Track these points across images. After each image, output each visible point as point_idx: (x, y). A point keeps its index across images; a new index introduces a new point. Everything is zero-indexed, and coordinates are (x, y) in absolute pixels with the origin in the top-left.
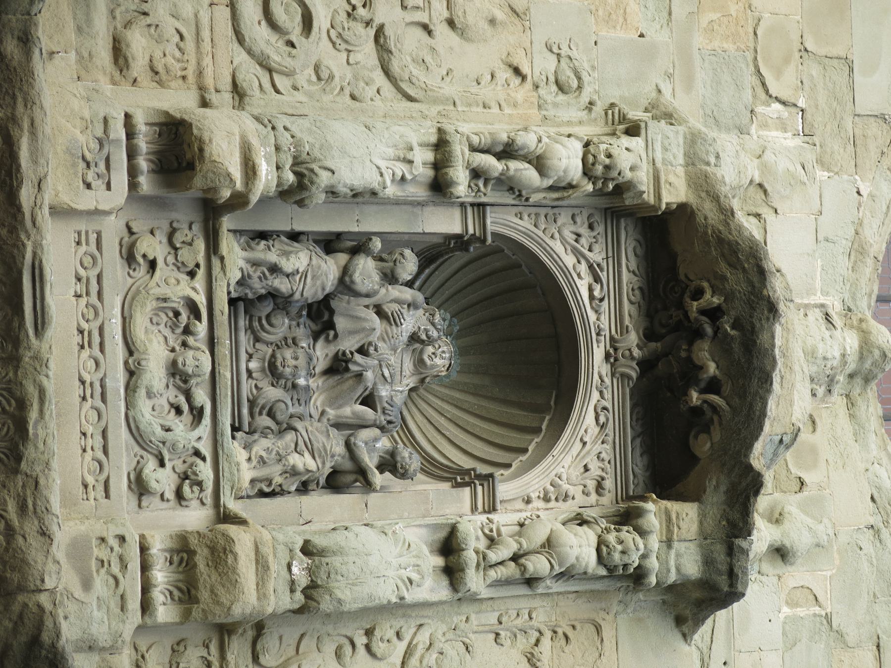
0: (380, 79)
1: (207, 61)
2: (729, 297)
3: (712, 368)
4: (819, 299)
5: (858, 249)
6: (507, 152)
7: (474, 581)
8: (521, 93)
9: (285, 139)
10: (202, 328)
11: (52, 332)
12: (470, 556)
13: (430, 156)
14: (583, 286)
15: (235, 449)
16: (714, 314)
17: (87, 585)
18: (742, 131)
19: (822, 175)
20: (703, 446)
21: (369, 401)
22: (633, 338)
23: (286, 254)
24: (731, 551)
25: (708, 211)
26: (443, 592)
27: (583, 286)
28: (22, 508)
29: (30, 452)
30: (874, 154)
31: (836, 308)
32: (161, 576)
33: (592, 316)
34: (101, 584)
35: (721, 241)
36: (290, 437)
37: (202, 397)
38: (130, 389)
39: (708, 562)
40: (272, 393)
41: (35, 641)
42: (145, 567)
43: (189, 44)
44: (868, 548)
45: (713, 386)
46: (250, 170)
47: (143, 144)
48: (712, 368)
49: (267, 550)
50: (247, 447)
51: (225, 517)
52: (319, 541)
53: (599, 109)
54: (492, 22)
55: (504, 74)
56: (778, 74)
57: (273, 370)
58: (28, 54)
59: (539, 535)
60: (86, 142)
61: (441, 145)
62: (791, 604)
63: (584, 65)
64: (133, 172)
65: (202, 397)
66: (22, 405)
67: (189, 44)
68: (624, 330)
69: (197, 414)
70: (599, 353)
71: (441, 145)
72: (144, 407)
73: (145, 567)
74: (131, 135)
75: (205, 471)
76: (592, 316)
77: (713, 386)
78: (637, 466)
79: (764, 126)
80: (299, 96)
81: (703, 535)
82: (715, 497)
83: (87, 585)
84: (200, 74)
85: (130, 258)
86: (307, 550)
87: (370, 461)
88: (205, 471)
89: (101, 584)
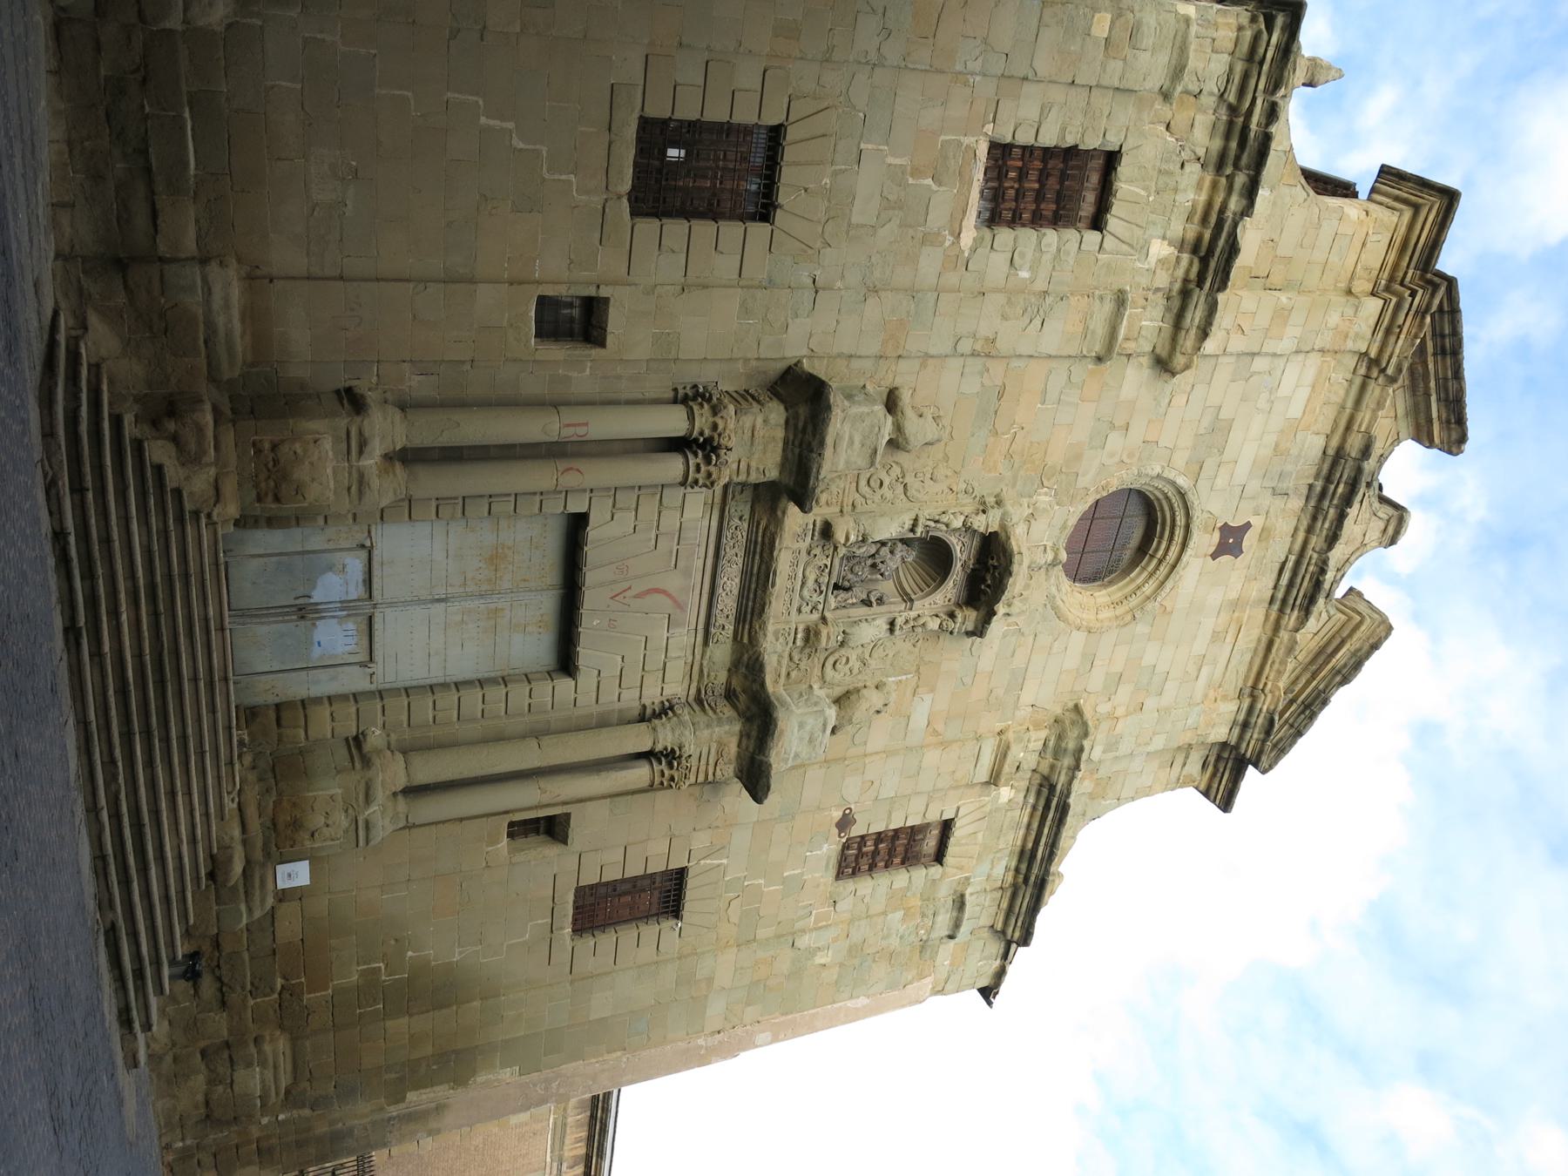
0: (903, 496)
1: (845, 499)
2: (1000, 564)
3: (989, 582)
4: (1045, 543)
5: (1064, 527)
6: (937, 522)
7: (897, 632)
8: (951, 497)
9: (862, 528)
10: (827, 571)
11: (777, 588)
12: (898, 627)
13: (912, 522)
14: (958, 549)
15: (831, 599)
16: (995, 568)
17: (777, 640)
18: (1030, 497)
19: (1057, 507)
20: (983, 598)
21: (882, 575)
22: (972, 561)
23: (860, 547)
24: (983, 626)
25: (1003, 535)
26: (888, 634)
27: (958, 549)
28: (760, 627)
29: (764, 616)
30: (1079, 498)
31: (1049, 544)
32: (799, 636)
33: (959, 555)
34: (781, 640)
35: (1003, 546)
36: (850, 593)
37: (824, 588)
38: (802, 587)
39: (976, 627)
40: (850, 576)
41: (757, 659)
42: (796, 633)
43: (841, 495)
44: (1040, 609)
45: (989, 586)
46: (847, 539)
47: (817, 529)
48: (989, 582)
49: (831, 634)
50: (836, 597)
51: (824, 619)
52: (847, 631)
53: (978, 499)
54: (946, 476)
55: (947, 490)
56: (1049, 480)
57: (851, 570)
58: (784, 516)
59: (921, 621)
60: (799, 530)
61: (916, 520)
62: (1008, 626)
63: (976, 484)
64: (813, 535)
65: (824, 588)
66: (765, 604)
67: (841, 495)
68: (969, 559)
69: (821, 592)
70: (959, 565)
71: (916, 520)
72: (806, 593)
73: (796, 633)
74: (814, 525)
75: (820, 607)
76: (959, 555)
77: (989, 586)
78: (963, 594)
79: (1040, 495)
80: (874, 505)
81: (976, 620)
82: (983, 612)
83: (777, 640)
84: (842, 502)
85: (809, 554)
86: (844, 632)
87: (873, 600)
88: (820, 607)
89: (781, 640)
